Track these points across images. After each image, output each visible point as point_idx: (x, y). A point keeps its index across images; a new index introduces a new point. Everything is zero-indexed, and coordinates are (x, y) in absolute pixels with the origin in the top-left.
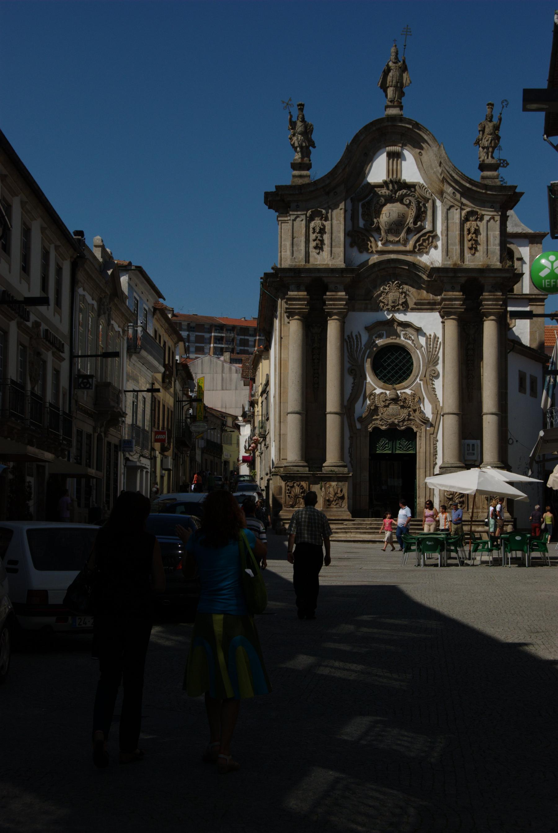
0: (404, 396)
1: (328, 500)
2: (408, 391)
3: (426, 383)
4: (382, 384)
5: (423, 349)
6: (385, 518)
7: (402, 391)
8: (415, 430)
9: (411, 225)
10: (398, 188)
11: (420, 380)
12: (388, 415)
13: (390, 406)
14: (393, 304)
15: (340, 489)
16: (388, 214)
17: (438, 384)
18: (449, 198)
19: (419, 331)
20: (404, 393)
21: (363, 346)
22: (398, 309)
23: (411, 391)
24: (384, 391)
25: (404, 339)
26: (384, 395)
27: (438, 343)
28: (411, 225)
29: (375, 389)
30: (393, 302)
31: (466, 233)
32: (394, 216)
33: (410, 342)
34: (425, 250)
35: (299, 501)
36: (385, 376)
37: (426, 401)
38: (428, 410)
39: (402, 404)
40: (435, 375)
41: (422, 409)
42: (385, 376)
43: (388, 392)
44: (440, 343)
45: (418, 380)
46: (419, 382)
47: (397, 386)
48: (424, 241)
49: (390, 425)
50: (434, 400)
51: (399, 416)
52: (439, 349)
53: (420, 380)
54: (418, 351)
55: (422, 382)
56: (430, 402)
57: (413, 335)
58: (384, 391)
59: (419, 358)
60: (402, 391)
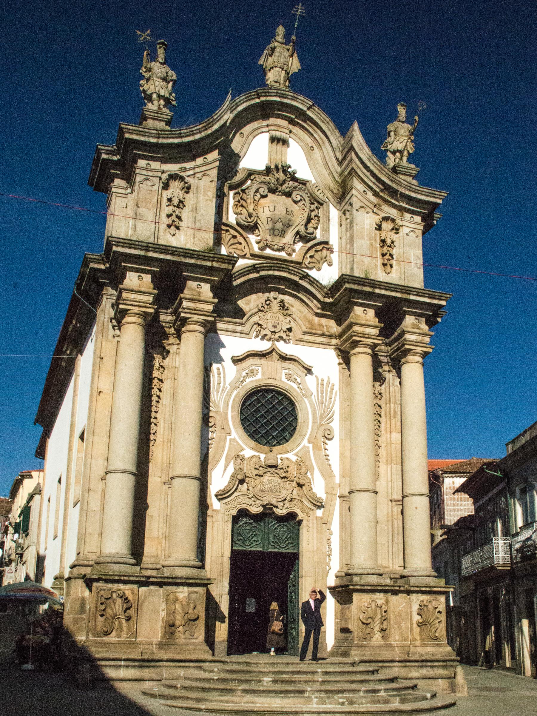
0: (286, 463)
1: (172, 625)
2: (292, 457)
3: (316, 447)
4: (253, 443)
5: (313, 396)
6: (492, 540)
7: (284, 456)
8: (301, 516)
9: (302, 229)
10: (280, 180)
11: (309, 442)
12: (263, 491)
13: (267, 477)
14: (273, 330)
15: (192, 606)
16: (272, 209)
17: (334, 448)
18: (360, 196)
19: (309, 371)
20: (287, 458)
21: (227, 385)
22: (281, 338)
23: (296, 458)
24: (257, 454)
25: (286, 381)
26: (258, 460)
27: (334, 392)
28: (302, 229)
29: (243, 449)
30: (274, 327)
31: (378, 244)
32: (281, 211)
33: (295, 386)
34: (317, 266)
35: (120, 624)
36: (257, 431)
37: (317, 472)
38: (319, 487)
39: (284, 475)
40: (330, 437)
41: (312, 486)
42: (257, 431)
43: (262, 456)
44: (336, 392)
45: (305, 442)
46: (307, 445)
47: (275, 449)
48: (316, 251)
49: (264, 506)
50: (327, 474)
51: (278, 493)
52: (335, 400)
53: (309, 442)
54: (306, 400)
55: (311, 446)
56: (323, 475)
57: (299, 376)
58: (257, 454)
59: (306, 412)
60: (284, 456)
